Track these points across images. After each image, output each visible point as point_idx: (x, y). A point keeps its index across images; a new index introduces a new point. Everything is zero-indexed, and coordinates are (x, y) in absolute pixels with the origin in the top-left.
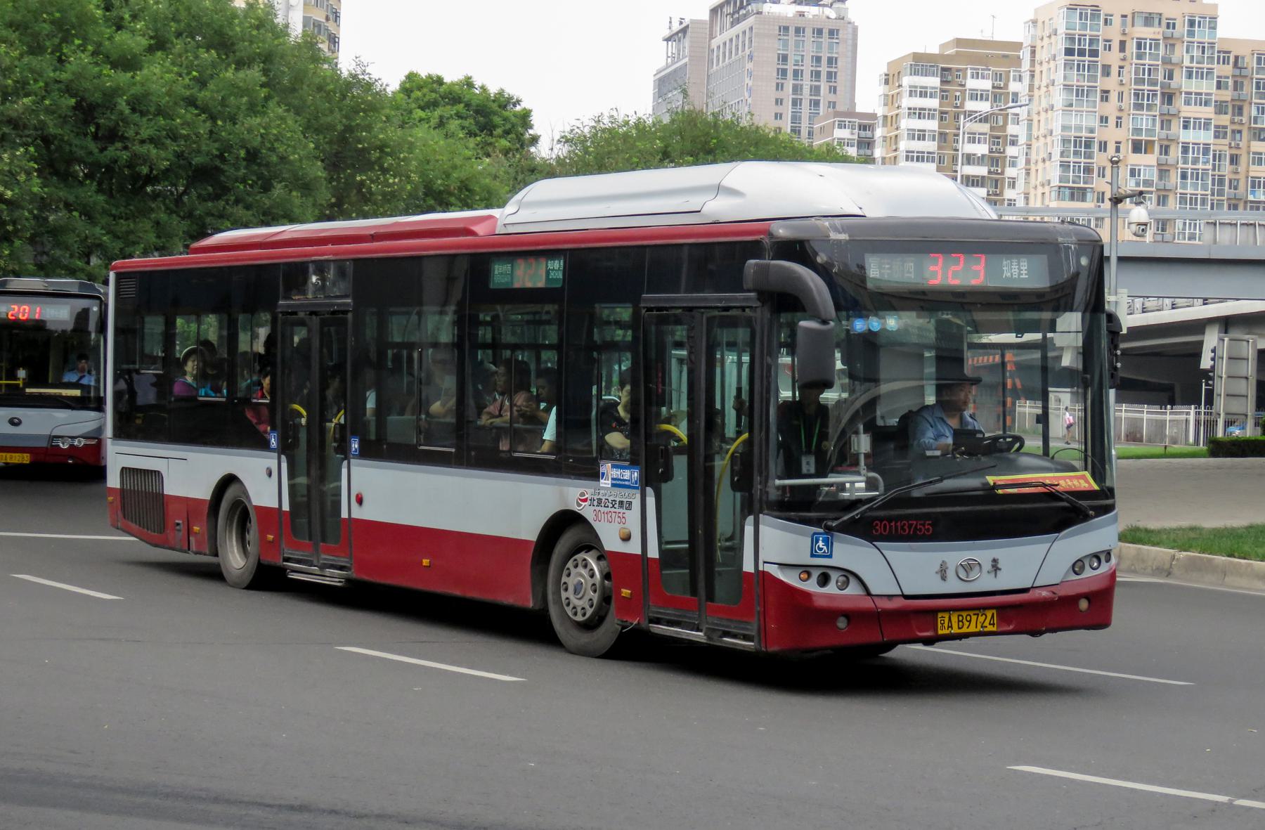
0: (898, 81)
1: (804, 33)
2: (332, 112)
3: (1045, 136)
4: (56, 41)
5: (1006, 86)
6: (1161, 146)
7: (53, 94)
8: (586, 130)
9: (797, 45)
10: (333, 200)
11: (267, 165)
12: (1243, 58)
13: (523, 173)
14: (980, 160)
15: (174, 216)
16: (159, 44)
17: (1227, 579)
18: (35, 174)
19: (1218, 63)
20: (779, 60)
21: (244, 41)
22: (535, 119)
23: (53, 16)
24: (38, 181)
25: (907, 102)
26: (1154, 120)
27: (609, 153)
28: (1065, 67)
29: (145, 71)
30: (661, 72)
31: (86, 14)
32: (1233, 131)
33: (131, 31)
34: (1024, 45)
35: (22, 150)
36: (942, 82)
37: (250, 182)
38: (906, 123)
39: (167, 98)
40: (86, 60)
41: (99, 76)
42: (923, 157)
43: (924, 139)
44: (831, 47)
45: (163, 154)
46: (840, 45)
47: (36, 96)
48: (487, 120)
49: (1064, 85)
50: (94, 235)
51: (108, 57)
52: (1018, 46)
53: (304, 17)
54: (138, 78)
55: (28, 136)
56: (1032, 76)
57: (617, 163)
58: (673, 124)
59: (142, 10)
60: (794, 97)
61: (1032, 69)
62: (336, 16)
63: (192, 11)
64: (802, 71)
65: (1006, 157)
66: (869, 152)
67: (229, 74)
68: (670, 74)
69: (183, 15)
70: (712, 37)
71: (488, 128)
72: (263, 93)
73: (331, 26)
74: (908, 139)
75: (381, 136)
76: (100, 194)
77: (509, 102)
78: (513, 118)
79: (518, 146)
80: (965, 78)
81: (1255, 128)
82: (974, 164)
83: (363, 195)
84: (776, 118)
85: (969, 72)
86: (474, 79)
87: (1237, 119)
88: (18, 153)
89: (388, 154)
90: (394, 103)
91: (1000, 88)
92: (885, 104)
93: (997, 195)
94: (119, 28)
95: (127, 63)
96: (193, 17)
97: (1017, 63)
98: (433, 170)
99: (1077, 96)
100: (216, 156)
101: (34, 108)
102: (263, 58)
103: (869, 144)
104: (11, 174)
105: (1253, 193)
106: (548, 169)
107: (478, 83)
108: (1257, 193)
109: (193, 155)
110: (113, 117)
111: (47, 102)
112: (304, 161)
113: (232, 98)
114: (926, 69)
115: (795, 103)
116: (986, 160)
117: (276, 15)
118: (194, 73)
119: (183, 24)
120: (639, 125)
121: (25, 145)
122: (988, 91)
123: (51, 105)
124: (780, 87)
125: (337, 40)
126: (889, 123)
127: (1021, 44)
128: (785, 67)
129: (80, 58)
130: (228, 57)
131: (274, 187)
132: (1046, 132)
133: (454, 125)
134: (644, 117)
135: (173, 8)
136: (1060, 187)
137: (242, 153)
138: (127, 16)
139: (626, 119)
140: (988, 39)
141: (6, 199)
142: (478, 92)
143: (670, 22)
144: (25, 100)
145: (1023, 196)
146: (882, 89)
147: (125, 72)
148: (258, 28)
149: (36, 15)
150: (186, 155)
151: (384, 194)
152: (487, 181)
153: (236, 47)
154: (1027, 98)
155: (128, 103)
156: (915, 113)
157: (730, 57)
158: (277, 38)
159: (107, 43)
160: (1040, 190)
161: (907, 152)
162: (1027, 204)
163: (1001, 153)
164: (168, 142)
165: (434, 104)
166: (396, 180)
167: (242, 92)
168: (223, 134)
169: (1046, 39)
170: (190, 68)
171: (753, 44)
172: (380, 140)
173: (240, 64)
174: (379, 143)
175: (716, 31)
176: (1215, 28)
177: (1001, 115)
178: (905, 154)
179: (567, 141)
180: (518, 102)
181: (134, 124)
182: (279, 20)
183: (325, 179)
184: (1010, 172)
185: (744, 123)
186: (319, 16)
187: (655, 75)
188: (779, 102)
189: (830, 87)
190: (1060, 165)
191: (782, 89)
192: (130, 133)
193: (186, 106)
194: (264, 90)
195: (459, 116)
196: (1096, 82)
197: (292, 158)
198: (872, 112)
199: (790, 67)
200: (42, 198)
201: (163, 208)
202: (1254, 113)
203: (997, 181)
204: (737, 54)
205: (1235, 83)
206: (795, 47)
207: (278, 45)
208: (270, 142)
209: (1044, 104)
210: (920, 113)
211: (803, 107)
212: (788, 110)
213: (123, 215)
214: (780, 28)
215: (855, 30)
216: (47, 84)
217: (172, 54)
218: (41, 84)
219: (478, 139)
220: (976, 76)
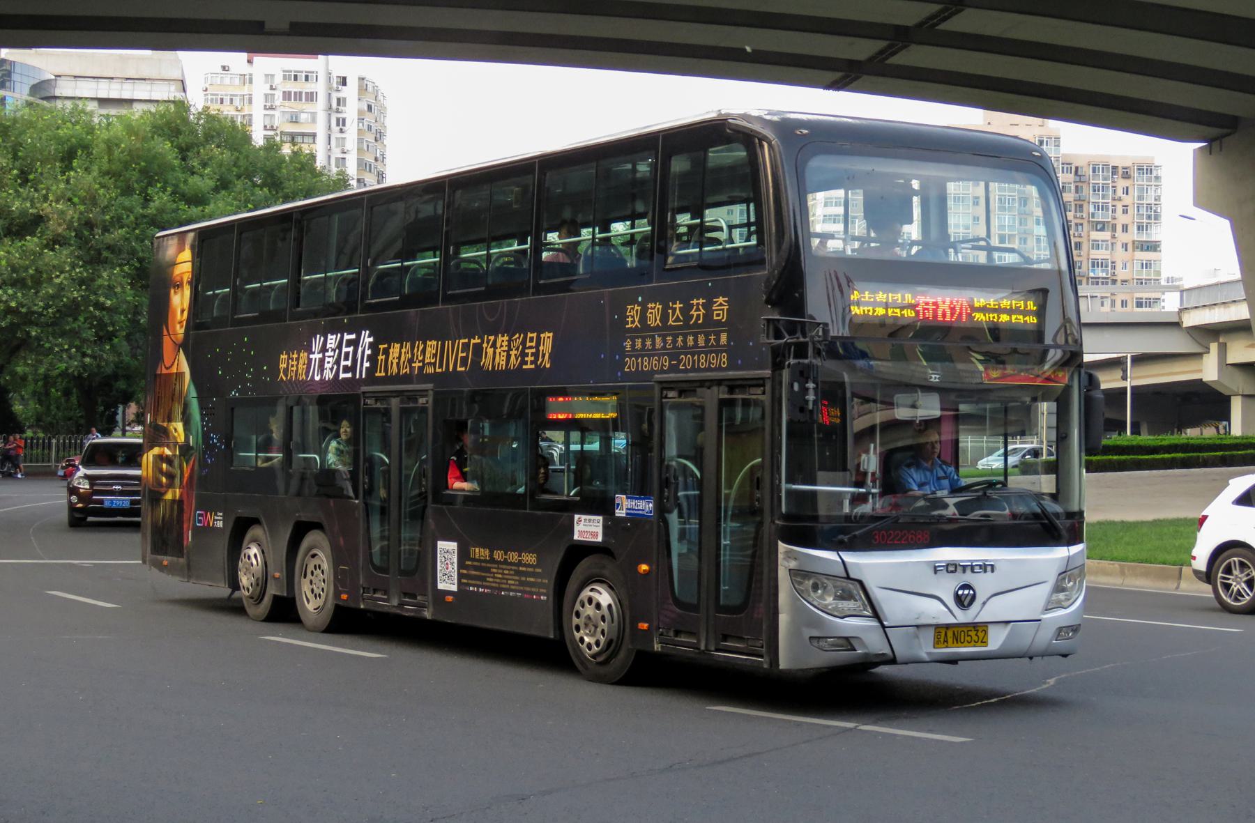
6: (1020, 239)
7: (142, 226)
12: (1082, 168)
16: (223, 185)
19: (1063, 172)
21: (289, 180)
23: (139, 164)
24: (132, 292)
26: (1014, 219)
29: (212, 206)
32: (1076, 225)
35: (118, 269)
47: (128, 227)
55: (123, 259)
59: (210, 159)
63: (250, 160)
69: (242, 162)
73: (379, 165)
81: (1093, 222)
87: (1078, 215)
94: (193, 173)
99: (955, 201)
104: (111, 288)
105: (1093, 271)
108: (1096, 271)
111: (137, 231)
119: (242, 169)
121: (121, 265)
129: (162, 199)
130: (277, 193)
135: (233, 157)
144: (120, 231)
147: (196, 207)
148: (300, 170)
149: (126, 165)
176: (1058, 146)
182: (320, 162)
186: (369, 159)
196: (969, 190)
200: (136, 306)
202: (1092, 210)
205: (1077, 187)
207: (316, 182)
216: (136, 219)
217: (234, 192)
218: (132, 218)
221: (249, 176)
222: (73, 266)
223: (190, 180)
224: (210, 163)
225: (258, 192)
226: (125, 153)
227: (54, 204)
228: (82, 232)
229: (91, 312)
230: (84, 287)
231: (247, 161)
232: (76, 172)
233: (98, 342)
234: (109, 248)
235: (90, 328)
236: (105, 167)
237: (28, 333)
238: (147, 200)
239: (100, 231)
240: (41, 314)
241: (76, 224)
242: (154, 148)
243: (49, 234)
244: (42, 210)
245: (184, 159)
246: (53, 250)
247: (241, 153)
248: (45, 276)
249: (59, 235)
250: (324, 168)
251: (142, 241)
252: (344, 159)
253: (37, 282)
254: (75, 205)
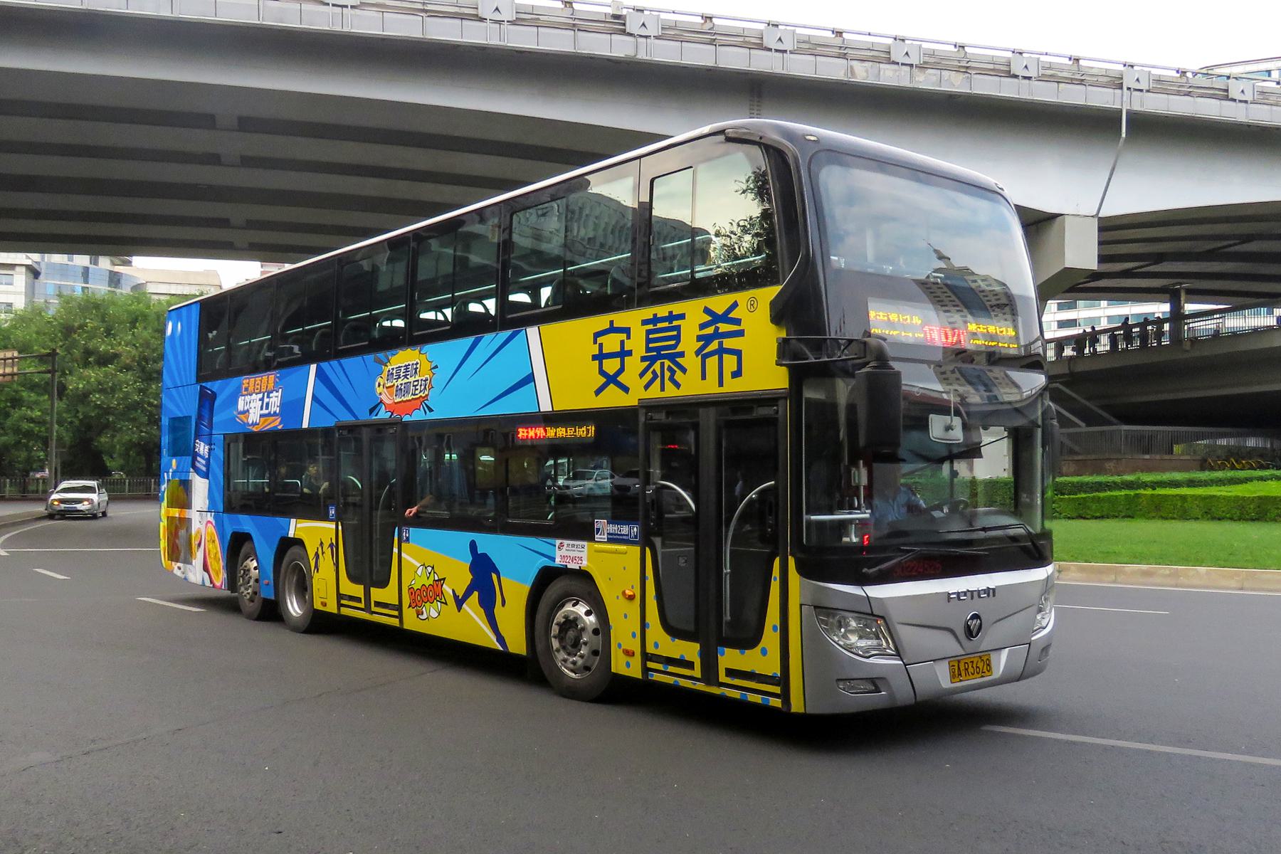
239: (151, 363)
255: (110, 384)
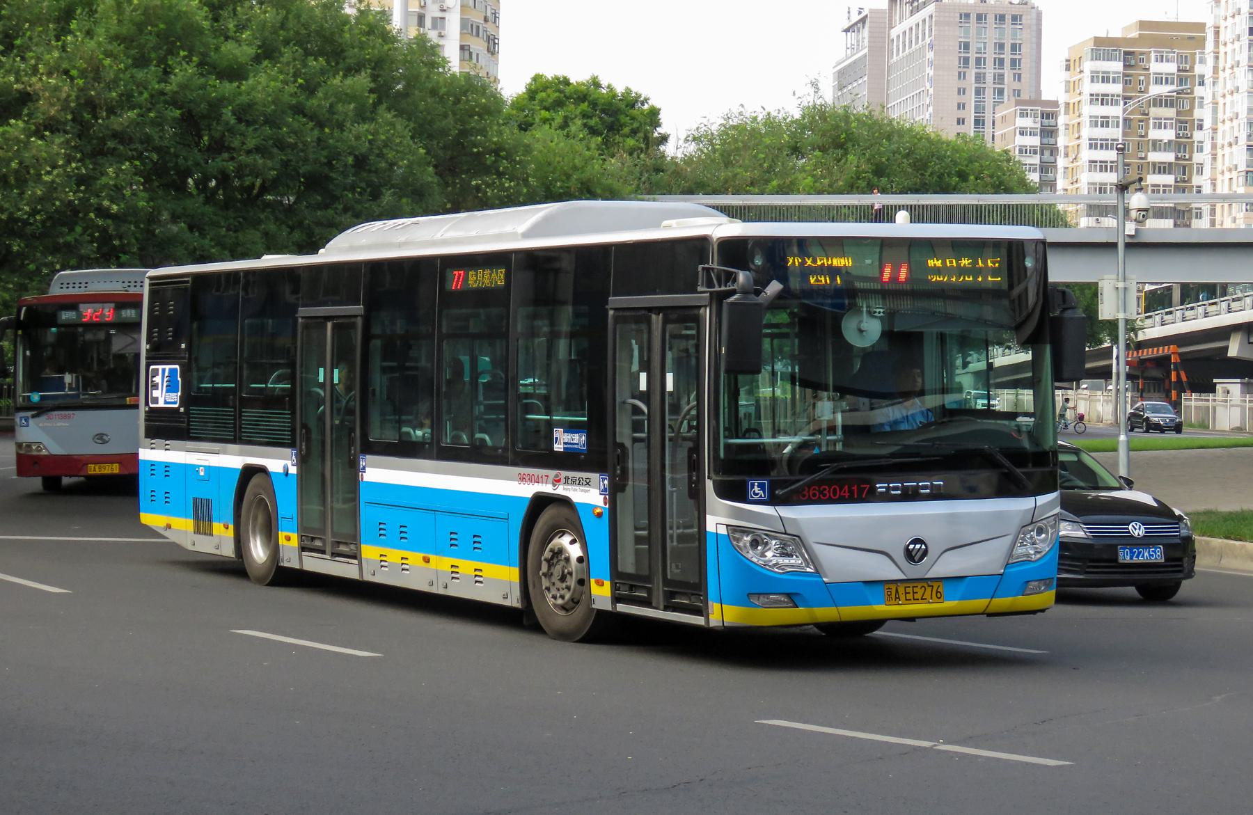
0: (1080, 66)
1: (985, 19)
2: (445, 116)
3: (1231, 120)
4: (162, 53)
5: (1192, 68)
7: (158, 106)
8: (715, 128)
9: (979, 33)
10: (449, 206)
11: (376, 171)
13: (647, 171)
14: (1168, 146)
15: (284, 227)
16: (267, 53)
17: (1223, 561)
18: (141, 187)
20: (960, 48)
21: (353, 48)
22: (663, 117)
23: (157, 26)
25: (1088, 88)
27: (737, 149)
28: (1250, 48)
29: (251, 81)
30: (840, 63)
31: (192, 25)
33: (237, 41)
34: (1207, 26)
35: (127, 163)
36: (1125, 66)
37: (359, 190)
38: (1088, 110)
39: (273, 107)
40: (190, 70)
41: (203, 87)
42: (1107, 145)
43: (1107, 126)
44: (1014, 34)
45: (269, 163)
46: (1024, 31)
47: (141, 109)
48: (612, 119)
49: (1249, 66)
50: (202, 246)
51: (215, 68)
52: (1201, 27)
53: (461, 19)
54: (243, 88)
56: (1217, 58)
57: (744, 160)
58: (804, 119)
59: (249, 20)
60: (977, 85)
61: (1217, 50)
62: (493, 18)
64: (985, 59)
65: (1194, 142)
66: (1052, 141)
67: (337, 81)
68: (850, 65)
69: (291, 24)
70: (891, 27)
71: (614, 128)
72: (372, 98)
74: (1091, 126)
75: (495, 139)
76: (207, 206)
77: (637, 101)
78: (641, 118)
79: (643, 146)
80: (1149, 61)
82: (1160, 150)
83: (481, 200)
84: (959, 108)
85: (1153, 55)
86: (600, 78)
88: (123, 167)
89: (503, 158)
90: (518, 105)
91: (1187, 71)
92: (1066, 92)
93: (1185, 182)
94: (227, 38)
95: (235, 73)
96: (303, 25)
97: (1201, 43)
98: (553, 173)
100: (325, 164)
101: (139, 119)
102: (373, 64)
103: (1052, 132)
104: (118, 188)
106: (673, 167)
107: (604, 83)
109: (301, 163)
110: (219, 128)
111: (152, 115)
112: (415, 166)
113: (340, 105)
114: (1108, 54)
115: (978, 92)
116: (1173, 145)
117: (389, 21)
118: (300, 81)
120: (770, 122)
121: (131, 159)
122: (1174, 74)
123: (156, 117)
124: (962, 76)
125: (496, 41)
126: (1071, 111)
127: (1204, 25)
128: (967, 55)
130: (337, 63)
131: (384, 195)
132: (1231, 115)
133: (576, 125)
134: (775, 114)
135: (280, 17)
136: (1247, 172)
137: (350, 160)
138: (231, 26)
139: (755, 115)
140: (1173, 20)
141: (112, 214)
142: (604, 91)
143: (849, 12)
144: (132, 114)
145: (1209, 181)
146: (1064, 75)
147: (231, 82)
149: (140, 27)
150: (292, 163)
151: (500, 198)
152: (610, 181)
153: (346, 54)
154: (1211, 80)
155: (234, 113)
156: (1098, 99)
157: (910, 47)
158: (387, 44)
159: (212, 53)
160: (1227, 175)
161: (1090, 140)
162: (1214, 190)
163: (1188, 138)
164: (275, 150)
165: (559, 104)
166: (512, 184)
167: (349, 98)
168: (331, 141)
169: (1229, 18)
170: (296, 75)
171: (933, 33)
172: (495, 143)
173: (350, 71)
174: (493, 146)
175: (895, 20)
177: (1187, 98)
178: (1088, 142)
179: (694, 139)
180: (646, 100)
181: (241, 134)
183: (439, 185)
184: (1197, 158)
185: (876, 114)
187: (834, 67)
188: (961, 91)
189: (1014, 75)
190: (1247, 149)
191: (964, 78)
192: (236, 143)
193: (294, 115)
194: (372, 96)
195: (584, 115)
197: (401, 163)
198: (1053, 98)
199: (972, 56)
201: (271, 217)
203: (1184, 167)
204: (917, 43)
206: (977, 34)
207: (390, 49)
208: (379, 148)
209: (1229, 87)
210: (1103, 99)
211: (986, 96)
212: (971, 98)
213: (232, 227)
214: (961, 15)
215: (1039, 16)
216: (152, 96)
217: (279, 62)
218: (146, 95)
219: (600, 139)
220: (1161, 59)
221: (299, 43)
222: (69, 160)
223: (223, 49)
224: (249, 24)
225: (312, 63)
226: (138, 12)
227: (44, 78)
228: (82, 116)
229: (91, 220)
230: (83, 188)
231: (299, 22)
232: (76, 36)
233: (102, 260)
234: (115, 135)
235: (92, 242)
236: (114, 28)
237: (10, 246)
238: (167, 73)
239: (104, 114)
240: (26, 223)
241: (73, 105)
242: (177, 5)
243: (40, 118)
244: (30, 86)
245: (216, 19)
246: (42, 138)
247: (288, 12)
248: (32, 171)
249: (51, 118)
250: (400, 31)
251: (160, 125)
252: (444, 18)
253: (22, 178)
254: (72, 79)
255: (14, 165)
